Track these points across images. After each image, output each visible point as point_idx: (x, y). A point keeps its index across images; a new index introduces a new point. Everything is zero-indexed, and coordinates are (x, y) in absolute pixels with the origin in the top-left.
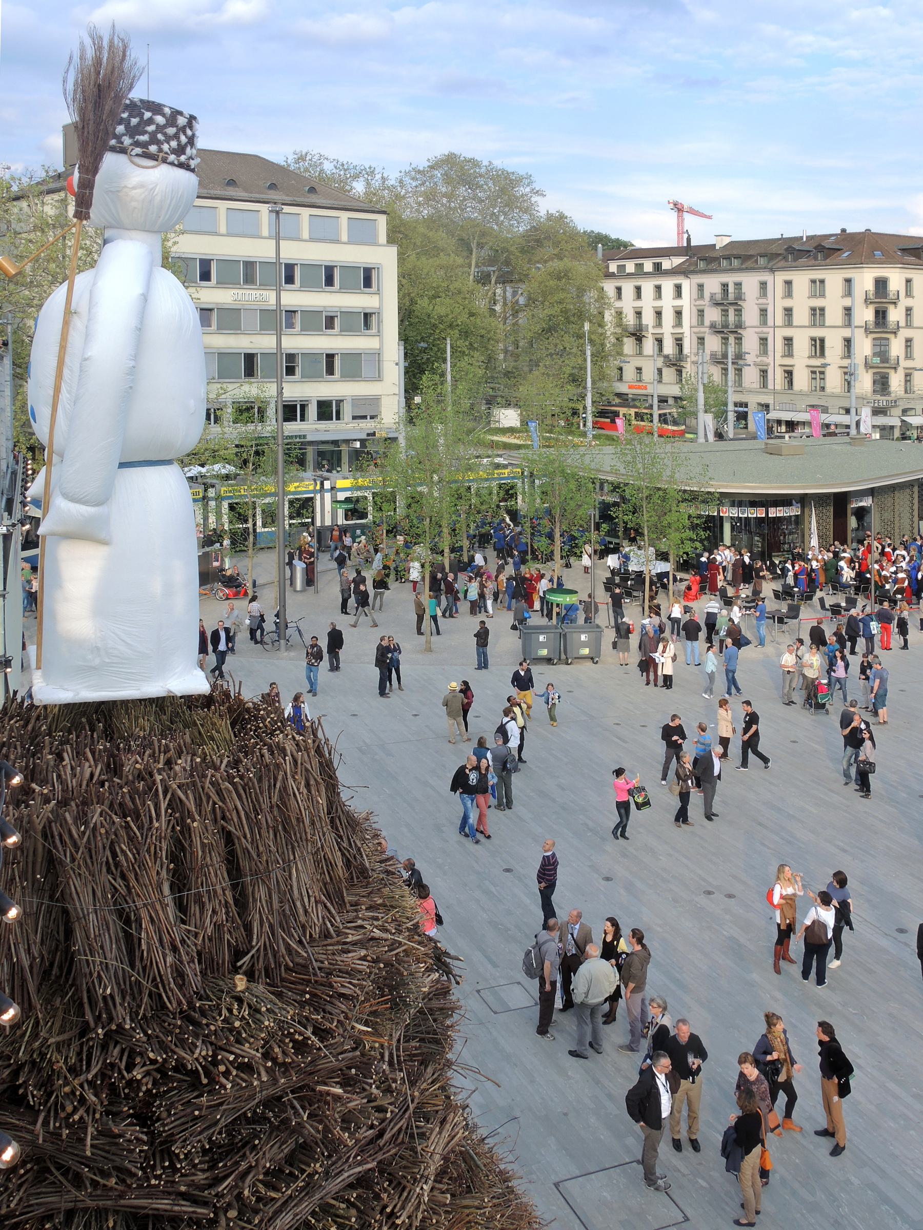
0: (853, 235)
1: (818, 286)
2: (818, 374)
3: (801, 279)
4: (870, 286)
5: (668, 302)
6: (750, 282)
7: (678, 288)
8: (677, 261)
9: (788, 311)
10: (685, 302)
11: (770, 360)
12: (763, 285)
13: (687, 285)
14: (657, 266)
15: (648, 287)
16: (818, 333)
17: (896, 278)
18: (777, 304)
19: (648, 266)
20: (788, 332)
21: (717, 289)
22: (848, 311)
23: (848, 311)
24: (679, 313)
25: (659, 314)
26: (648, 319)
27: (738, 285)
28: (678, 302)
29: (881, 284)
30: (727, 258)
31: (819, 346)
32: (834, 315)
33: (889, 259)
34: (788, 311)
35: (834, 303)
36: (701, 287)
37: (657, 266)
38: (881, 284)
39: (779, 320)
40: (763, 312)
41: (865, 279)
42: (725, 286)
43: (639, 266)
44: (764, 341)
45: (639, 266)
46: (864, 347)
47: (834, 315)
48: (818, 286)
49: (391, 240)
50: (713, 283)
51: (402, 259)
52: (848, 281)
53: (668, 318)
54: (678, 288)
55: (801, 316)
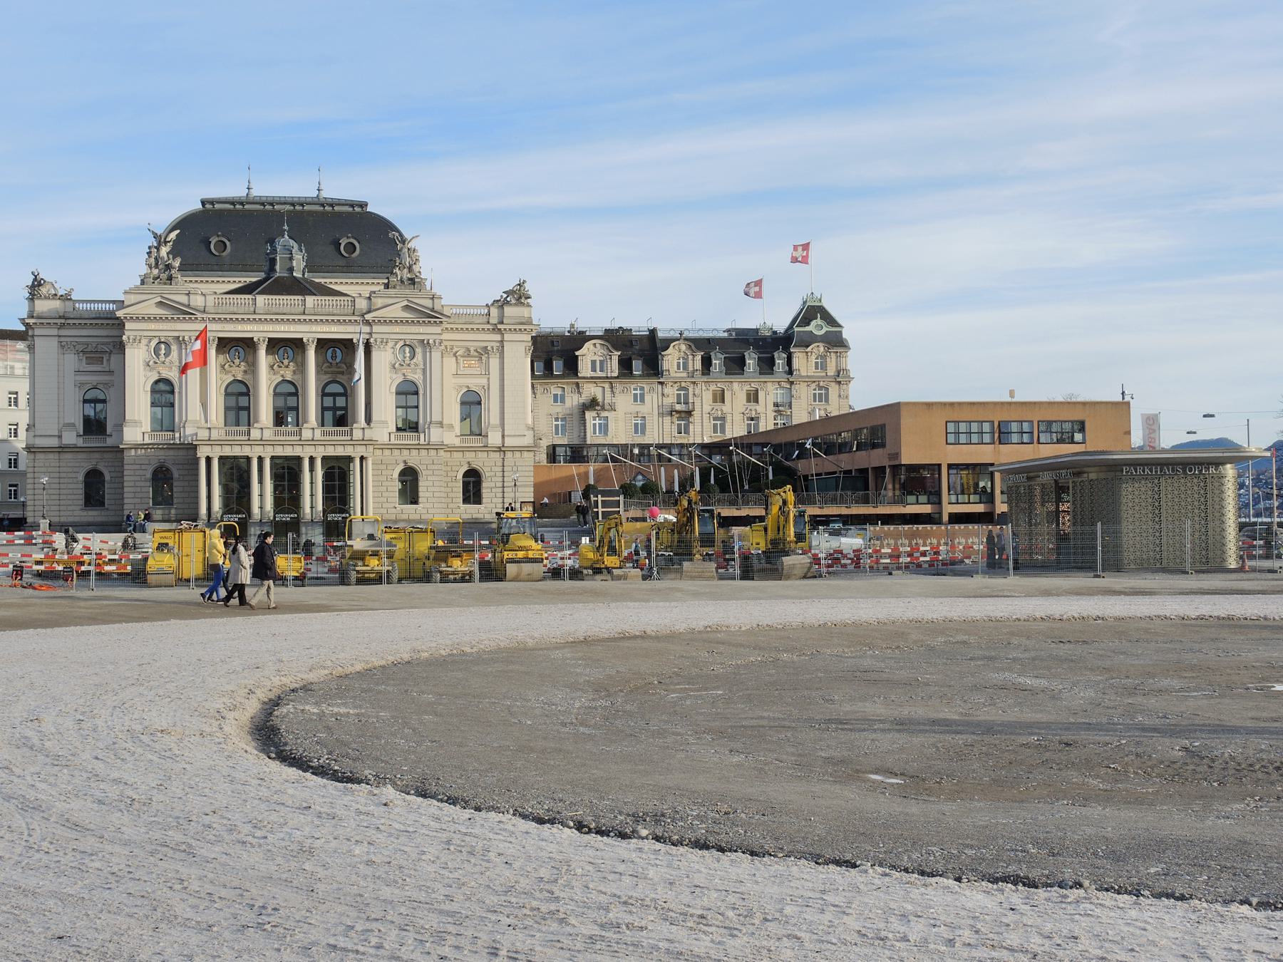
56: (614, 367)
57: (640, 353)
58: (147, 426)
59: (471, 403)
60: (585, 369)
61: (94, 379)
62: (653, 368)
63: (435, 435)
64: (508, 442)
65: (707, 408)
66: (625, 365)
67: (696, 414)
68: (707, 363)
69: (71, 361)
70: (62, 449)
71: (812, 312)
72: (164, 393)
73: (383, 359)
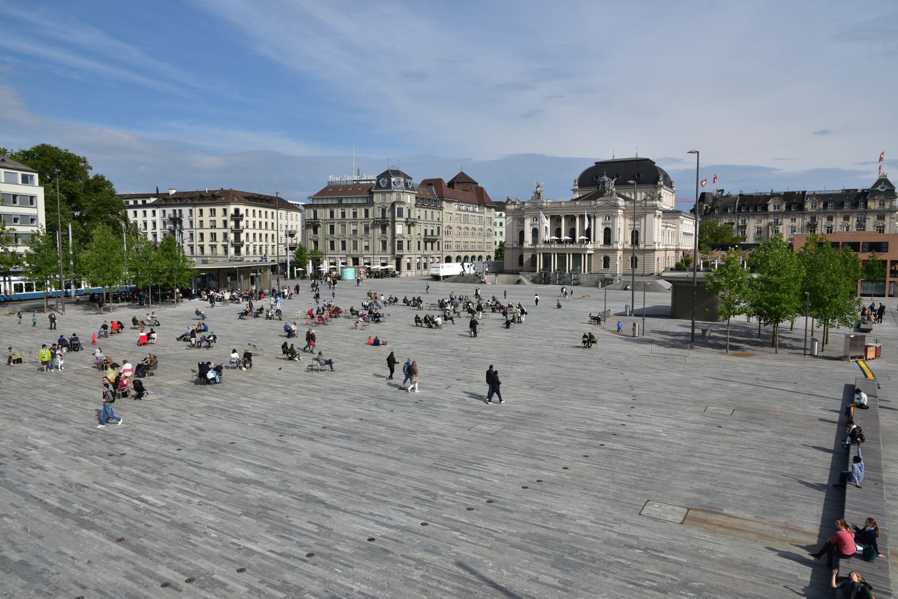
0: (226, 191)
1: (213, 213)
2: (213, 247)
3: (206, 210)
4: (233, 212)
5: (149, 218)
6: (185, 210)
7: (154, 212)
8: (153, 200)
9: (201, 222)
10: (158, 218)
11: (194, 243)
12: (191, 211)
13: (158, 211)
14: (144, 202)
15: (140, 211)
16: (213, 231)
17: (242, 209)
18: (196, 219)
19: (140, 202)
20: (201, 231)
21: (172, 212)
22: (225, 222)
23: (225, 222)
24: (154, 224)
25: (145, 224)
26: (140, 225)
27: (180, 211)
28: (154, 218)
29: (237, 211)
30: (175, 199)
31: (214, 236)
32: (220, 224)
33: (240, 202)
34: (201, 222)
35: (219, 218)
36: (164, 211)
37: (144, 202)
38: (237, 211)
39: (198, 226)
40: (191, 222)
41: (231, 209)
42: (175, 211)
43: (136, 202)
44: (192, 235)
45: (136, 202)
46: (232, 237)
47: (220, 224)
48: (213, 213)
49: (40, 185)
50: (169, 211)
51: (45, 191)
52: (225, 210)
53: (150, 226)
54: (154, 212)
55: (207, 224)
56: (784, 207)
57: (794, 202)
58: (530, 243)
59: (635, 235)
60: (771, 208)
61: (521, 228)
62: (801, 207)
63: (615, 246)
64: (647, 248)
65: (824, 223)
66: (788, 207)
67: (819, 226)
68: (825, 205)
69: (516, 222)
70: (513, 248)
71: (883, 181)
72: (535, 232)
73: (599, 221)
